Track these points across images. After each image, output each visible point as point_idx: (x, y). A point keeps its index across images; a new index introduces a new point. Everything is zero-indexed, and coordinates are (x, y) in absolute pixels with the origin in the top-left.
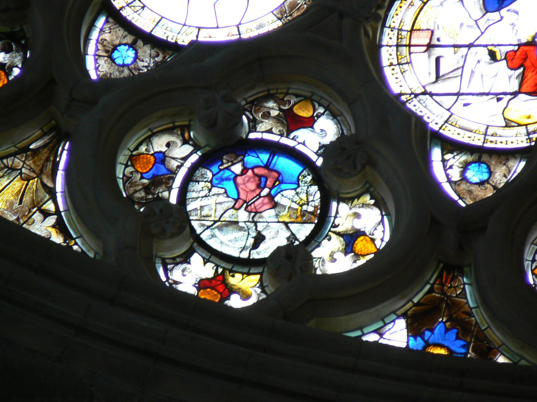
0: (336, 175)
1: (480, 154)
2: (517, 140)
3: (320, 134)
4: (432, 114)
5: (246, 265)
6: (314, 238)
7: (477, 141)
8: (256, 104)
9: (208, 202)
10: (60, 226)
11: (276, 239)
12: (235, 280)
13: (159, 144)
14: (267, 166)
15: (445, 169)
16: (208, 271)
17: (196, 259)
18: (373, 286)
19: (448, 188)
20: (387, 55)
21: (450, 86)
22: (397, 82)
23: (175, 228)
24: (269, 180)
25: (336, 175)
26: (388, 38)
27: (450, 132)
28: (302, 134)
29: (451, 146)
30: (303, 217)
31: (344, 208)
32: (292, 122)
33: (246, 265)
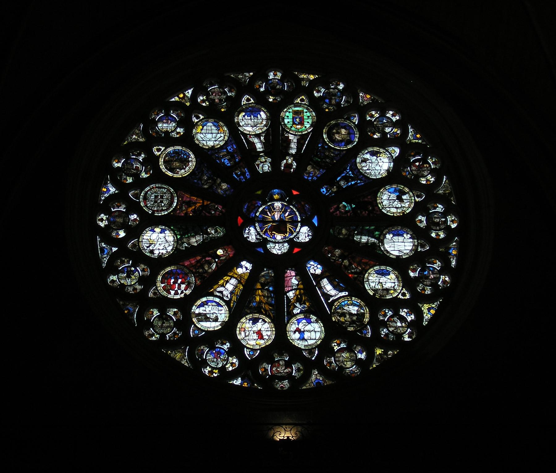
0: (230, 353)
1: (252, 350)
2: (258, 347)
3: (227, 346)
4: (244, 343)
5: (216, 369)
6: (226, 364)
7: (252, 347)
8: (217, 341)
9: (210, 357)
10: (187, 361)
11: (220, 365)
12: (214, 371)
13: (202, 348)
14: (219, 351)
15: (246, 352)
16: (210, 370)
17: (208, 367)
18: (234, 374)
19: (247, 355)
20: (238, 332)
21: (247, 338)
22: (239, 337)
23: (205, 363)
24: (219, 353)
25: (230, 353)
26: (238, 329)
27: (247, 346)
28: (225, 346)
29: (248, 348)
30: (225, 360)
31: (231, 358)
32: (223, 344)
33: (216, 369)
